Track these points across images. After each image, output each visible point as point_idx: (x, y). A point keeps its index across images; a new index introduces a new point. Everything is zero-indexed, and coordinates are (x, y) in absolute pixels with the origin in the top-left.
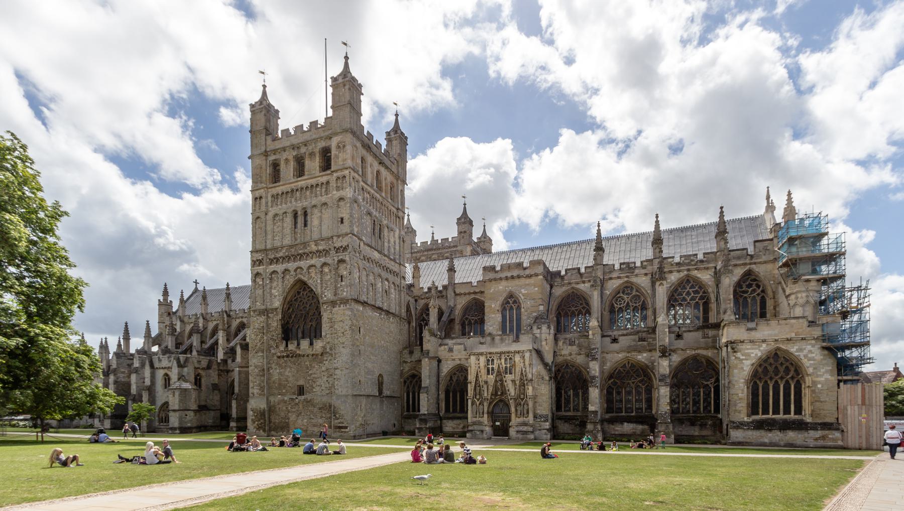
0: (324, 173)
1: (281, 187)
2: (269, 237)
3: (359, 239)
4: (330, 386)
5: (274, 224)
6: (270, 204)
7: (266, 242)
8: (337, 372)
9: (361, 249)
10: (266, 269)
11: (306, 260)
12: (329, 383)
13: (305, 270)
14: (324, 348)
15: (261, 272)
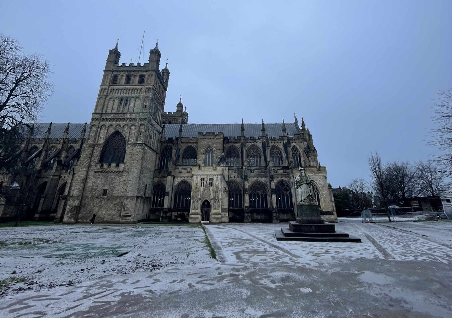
1: (117, 86)
4: (124, 190)
8: (130, 182)
12: (123, 189)
14: (124, 168)
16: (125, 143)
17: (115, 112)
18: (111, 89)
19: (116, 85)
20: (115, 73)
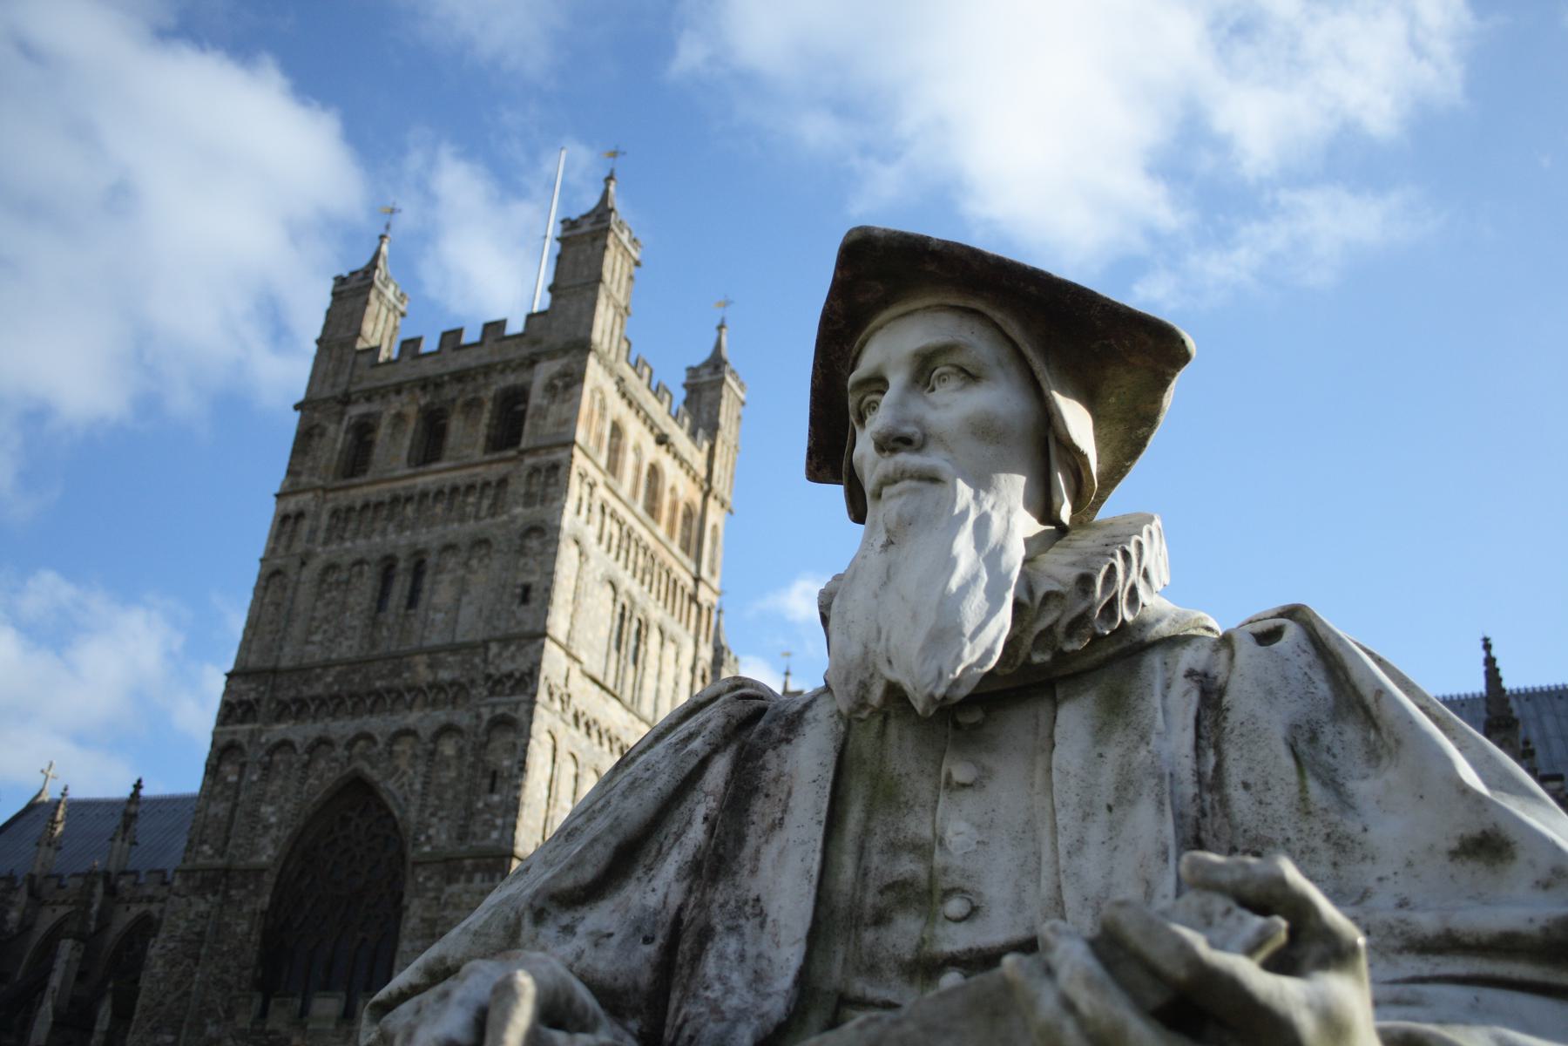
0: (497, 456)
2: (297, 630)
3: (569, 654)
5: (319, 595)
6: (321, 535)
7: (281, 648)
9: (572, 688)
10: (261, 732)
11: (392, 711)
13: (381, 746)
15: (242, 739)
16: (403, 856)
17: (351, 655)
18: (335, 513)
19: (356, 481)
20: (356, 411)
